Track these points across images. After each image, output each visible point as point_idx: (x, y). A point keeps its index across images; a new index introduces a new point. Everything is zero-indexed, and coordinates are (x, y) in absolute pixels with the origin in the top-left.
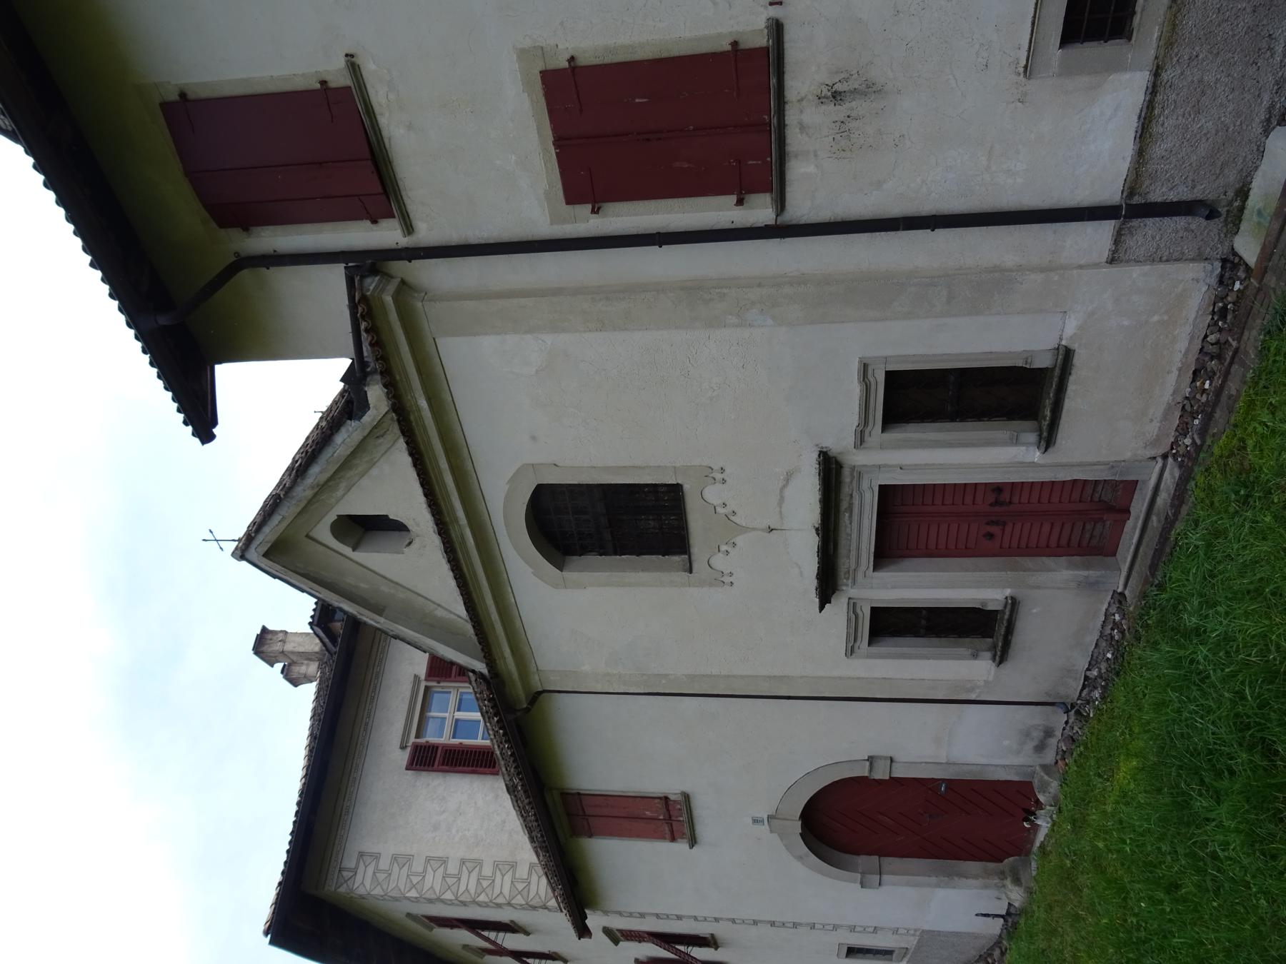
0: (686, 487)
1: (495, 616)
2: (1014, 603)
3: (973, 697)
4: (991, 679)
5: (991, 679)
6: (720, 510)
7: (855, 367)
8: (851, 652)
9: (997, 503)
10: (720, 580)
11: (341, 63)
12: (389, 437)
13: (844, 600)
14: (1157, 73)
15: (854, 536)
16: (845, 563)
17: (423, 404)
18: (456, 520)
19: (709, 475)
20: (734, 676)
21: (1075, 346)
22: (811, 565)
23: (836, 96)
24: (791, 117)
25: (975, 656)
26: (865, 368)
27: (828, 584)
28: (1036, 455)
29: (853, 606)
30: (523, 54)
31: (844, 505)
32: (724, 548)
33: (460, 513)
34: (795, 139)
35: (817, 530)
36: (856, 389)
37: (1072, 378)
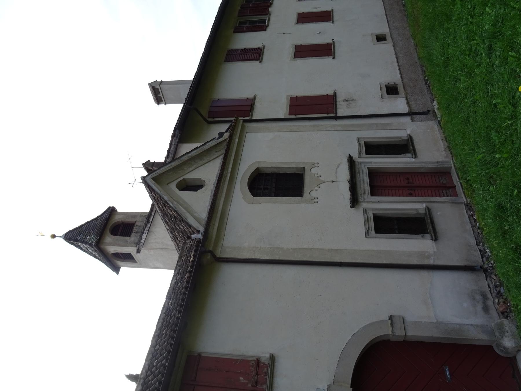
0: (306, 168)
1: (220, 208)
2: (428, 209)
3: (431, 262)
4: (436, 251)
5: (436, 251)
6: (316, 175)
7: (356, 140)
8: (367, 234)
9: (408, 183)
10: (313, 201)
11: (253, 96)
12: (219, 153)
13: (361, 209)
14: (406, 97)
15: (362, 182)
16: (360, 191)
17: (237, 140)
18: (228, 170)
19: (314, 165)
20: (314, 249)
21: (411, 135)
22: (347, 195)
23: (346, 101)
24: (338, 103)
25: (423, 238)
26: (358, 139)
27: (355, 201)
28: (414, 160)
29: (365, 211)
30: (288, 96)
31: (357, 171)
32: (316, 188)
33: (230, 169)
34: (338, 106)
35: (349, 182)
36: (357, 144)
37: (414, 142)
